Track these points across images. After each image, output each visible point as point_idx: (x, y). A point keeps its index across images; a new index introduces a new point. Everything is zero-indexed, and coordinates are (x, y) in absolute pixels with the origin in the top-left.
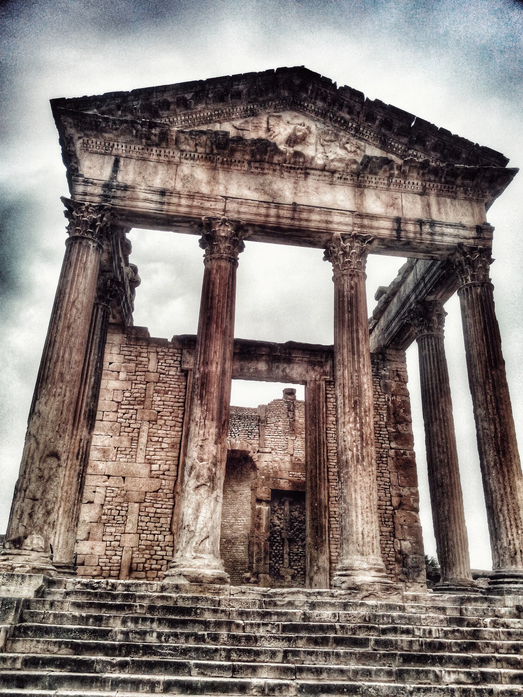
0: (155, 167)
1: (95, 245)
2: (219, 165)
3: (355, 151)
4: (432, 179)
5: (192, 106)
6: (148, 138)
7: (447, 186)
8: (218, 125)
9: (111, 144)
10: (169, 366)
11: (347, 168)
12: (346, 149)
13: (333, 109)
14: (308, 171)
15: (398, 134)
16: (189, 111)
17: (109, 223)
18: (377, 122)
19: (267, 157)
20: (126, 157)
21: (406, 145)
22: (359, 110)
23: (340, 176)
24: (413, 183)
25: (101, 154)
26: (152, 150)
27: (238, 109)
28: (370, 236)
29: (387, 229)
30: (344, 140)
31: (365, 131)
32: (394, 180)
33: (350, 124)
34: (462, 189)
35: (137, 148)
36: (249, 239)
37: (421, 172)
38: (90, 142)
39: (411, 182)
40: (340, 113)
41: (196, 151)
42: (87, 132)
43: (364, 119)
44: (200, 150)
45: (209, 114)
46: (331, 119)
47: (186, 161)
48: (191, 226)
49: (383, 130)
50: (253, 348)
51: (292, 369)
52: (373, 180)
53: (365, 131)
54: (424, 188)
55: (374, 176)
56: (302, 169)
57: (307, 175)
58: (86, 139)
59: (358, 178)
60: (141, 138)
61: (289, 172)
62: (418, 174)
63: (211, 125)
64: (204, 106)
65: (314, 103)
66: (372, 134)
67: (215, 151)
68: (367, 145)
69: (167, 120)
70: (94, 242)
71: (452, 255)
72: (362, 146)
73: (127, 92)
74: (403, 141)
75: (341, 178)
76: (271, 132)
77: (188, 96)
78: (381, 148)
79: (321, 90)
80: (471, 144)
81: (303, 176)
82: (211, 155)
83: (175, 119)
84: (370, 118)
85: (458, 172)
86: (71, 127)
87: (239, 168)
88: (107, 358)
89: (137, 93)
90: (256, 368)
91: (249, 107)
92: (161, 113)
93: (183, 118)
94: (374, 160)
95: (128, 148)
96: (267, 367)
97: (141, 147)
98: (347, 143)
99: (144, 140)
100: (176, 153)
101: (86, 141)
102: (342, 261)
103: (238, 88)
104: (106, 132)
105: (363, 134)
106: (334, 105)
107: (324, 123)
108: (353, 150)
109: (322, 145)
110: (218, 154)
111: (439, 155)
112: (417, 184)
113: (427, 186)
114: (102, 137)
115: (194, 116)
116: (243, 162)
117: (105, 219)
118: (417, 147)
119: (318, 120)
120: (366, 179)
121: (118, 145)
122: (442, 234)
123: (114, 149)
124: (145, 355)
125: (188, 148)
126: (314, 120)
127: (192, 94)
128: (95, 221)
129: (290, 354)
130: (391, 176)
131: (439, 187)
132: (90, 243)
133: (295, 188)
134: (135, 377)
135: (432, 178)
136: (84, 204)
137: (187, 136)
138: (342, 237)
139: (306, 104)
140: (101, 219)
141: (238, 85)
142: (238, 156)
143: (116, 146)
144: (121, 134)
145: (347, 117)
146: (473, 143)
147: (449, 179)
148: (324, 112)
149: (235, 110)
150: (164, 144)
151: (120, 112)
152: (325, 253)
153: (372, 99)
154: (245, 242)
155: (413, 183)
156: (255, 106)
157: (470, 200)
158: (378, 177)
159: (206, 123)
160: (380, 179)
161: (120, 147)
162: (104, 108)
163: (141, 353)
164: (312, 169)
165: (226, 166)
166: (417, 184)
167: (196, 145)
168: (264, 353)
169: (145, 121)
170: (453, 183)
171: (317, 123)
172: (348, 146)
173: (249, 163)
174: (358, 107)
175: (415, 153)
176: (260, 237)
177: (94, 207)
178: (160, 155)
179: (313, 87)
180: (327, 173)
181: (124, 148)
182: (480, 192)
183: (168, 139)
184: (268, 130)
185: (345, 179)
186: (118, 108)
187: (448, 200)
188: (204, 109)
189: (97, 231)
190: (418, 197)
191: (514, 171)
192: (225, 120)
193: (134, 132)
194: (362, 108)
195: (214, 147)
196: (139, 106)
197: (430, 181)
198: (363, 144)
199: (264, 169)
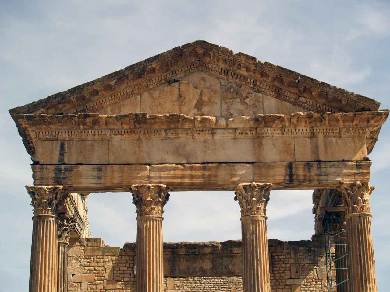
0: (92, 145)
1: (54, 219)
2: (142, 136)
3: (254, 104)
4: (318, 125)
5: (117, 88)
6: (84, 124)
7: (331, 128)
8: (139, 97)
9: (57, 133)
10: (124, 273)
11: (246, 125)
12: (247, 103)
13: (233, 68)
14: (215, 131)
15: (289, 86)
16: (115, 92)
17: (62, 197)
18: (270, 79)
19: (179, 125)
20: (70, 140)
21: (297, 94)
22: (254, 69)
23: (241, 132)
24: (303, 130)
25: (50, 140)
26: (88, 132)
27: (154, 81)
28: (267, 185)
29: (282, 175)
30: (244, 94)
31: (261, 85)
32: (286, 129)
33: (249, 80)
34: (344, 129)
35: (76, 133)
36: (171, 191)
37: (308, 122)
38: (41, 133)
39: (301, 129)
40: (239, 71)
41: (123, 128)
42: (38, 127)
43: (259, 76)
44: (125, 127)
45: (131, 90)
46: (232, 77)
47: (115, 137)
48: (125, 189)
49: (276, 83)
50: (197, 249)
51: (234, 265)
52: (269, 131)
53: (261, 85)
54: (313, 133)
55: (269, 129)
56: (209, 131)
57: (213, 134)
58: (38, 131)
59: (256, 131)
60: (79, 125)
61: (199, 134)
62: (306, 123)
63: (133, 98)
64: (126, 85)
65: (217, 65)
66: (268, 87)
67: (138, 126)
68: (264, 95)
69: (98, 103)
70: (53, 217)
71: (340, 187)
72: (259, 97)
73: (65, 92)
74: (293, 91)
75: (242, 133)
76: (183, 98)
77: (112, 83)
78: (276, 97)
79: (221, 56)
80: (347, 93)
81: (211, 135)
82: (134, 130)
83: (104, 100)
84: (263, 74)
85: (339, 118)
86: (25, 124)
87: (158, 136)
88: (70, 271)
89: (72, 91)
90: (202, 268)
91: (163, 78)
92: (92, 98)
93: (110, 98)
94: (267, 117)
95: (70, 134)
96: (211, 265)
97: (79, 132)
98: (247, 97)
99: (81, 127)
100: (107, 131)
101: (38, 133)
102: (245, 208)
103: (152, 67)
104: (51, 124)
105: (260, 87)
106: (234, 65)
107: (227, 80)
108: (252, 104)
109: (226, 103)
110: (140, 128)
111: (324, 101)
112: (306, 130)
113: (315, 131)
114: (50, 128)
115: (119, 95)
116: (161, 131)
117: (58, 196)
118: (305, 95)
119: (222, 78)
120: (263, 131)
121: (62, 132)
122: (327, 174)
123: (59, 136)
124: (102, 264)
125: (116, 127)
126: (218, 78)
127: (116, 80)
128: (52, 200)
129: (231, 251)
130: (284, 127)
131: (325, 130)
132: (51, 219)
133: (205, 147)
134: (94, 287)
135: (318, 125)
136: (42, 188)
137: (114, 119)
138: (244, 188)
139: (210, 66)
140: (56, 199)
141: (151, 65)
142: (156, 127)
143: (60, 133)
144: (64, 124)
145: (246, 74)
146: (349, 92)
147: (332, 123)
148: (226, 71)
149: (151, 82)
150: (97, 127)
151: (61, 105)
152: (236, 193)
153: (263, 62)
154: (170, 193)
155: (303, 130)
156: (168, 75)
157: (353, 137)
158: (272, 129)
159: (129, 97)
160: (274, 130)
161: (63, 133)
162: (49, 105)
163: (97, 263)
164: (218, 129)
165: (147, 136)
166: (306, 130)
167: (122, 123)
168: (206, 252)
169: (81, 115)
170: (336, 126)
171: (221, 80)
172: (247, 101)
173: (166, 131)
174: (253, 67)
175: (304, 101)
176: (180, 190)
177: (50, 189)
178: (95, 135)
179: (214, 55)
180: (231, 131)
181: (67, 134)
182: (360, 130)
183: (99, 122)
184: (180, 96)
185: (245, 133)
186: (60, 103)
187: (334, 140)
188: (126, 87)
189: (54, 207)
190: (309, 140)
191: (386, 114)
192: (145, 91)
193: (73, 122)
194: (256, 68)
195: (136, 124)
196: (75, 99)
197: (316, 126)
198: (260, 95)
199: (178, 134)
